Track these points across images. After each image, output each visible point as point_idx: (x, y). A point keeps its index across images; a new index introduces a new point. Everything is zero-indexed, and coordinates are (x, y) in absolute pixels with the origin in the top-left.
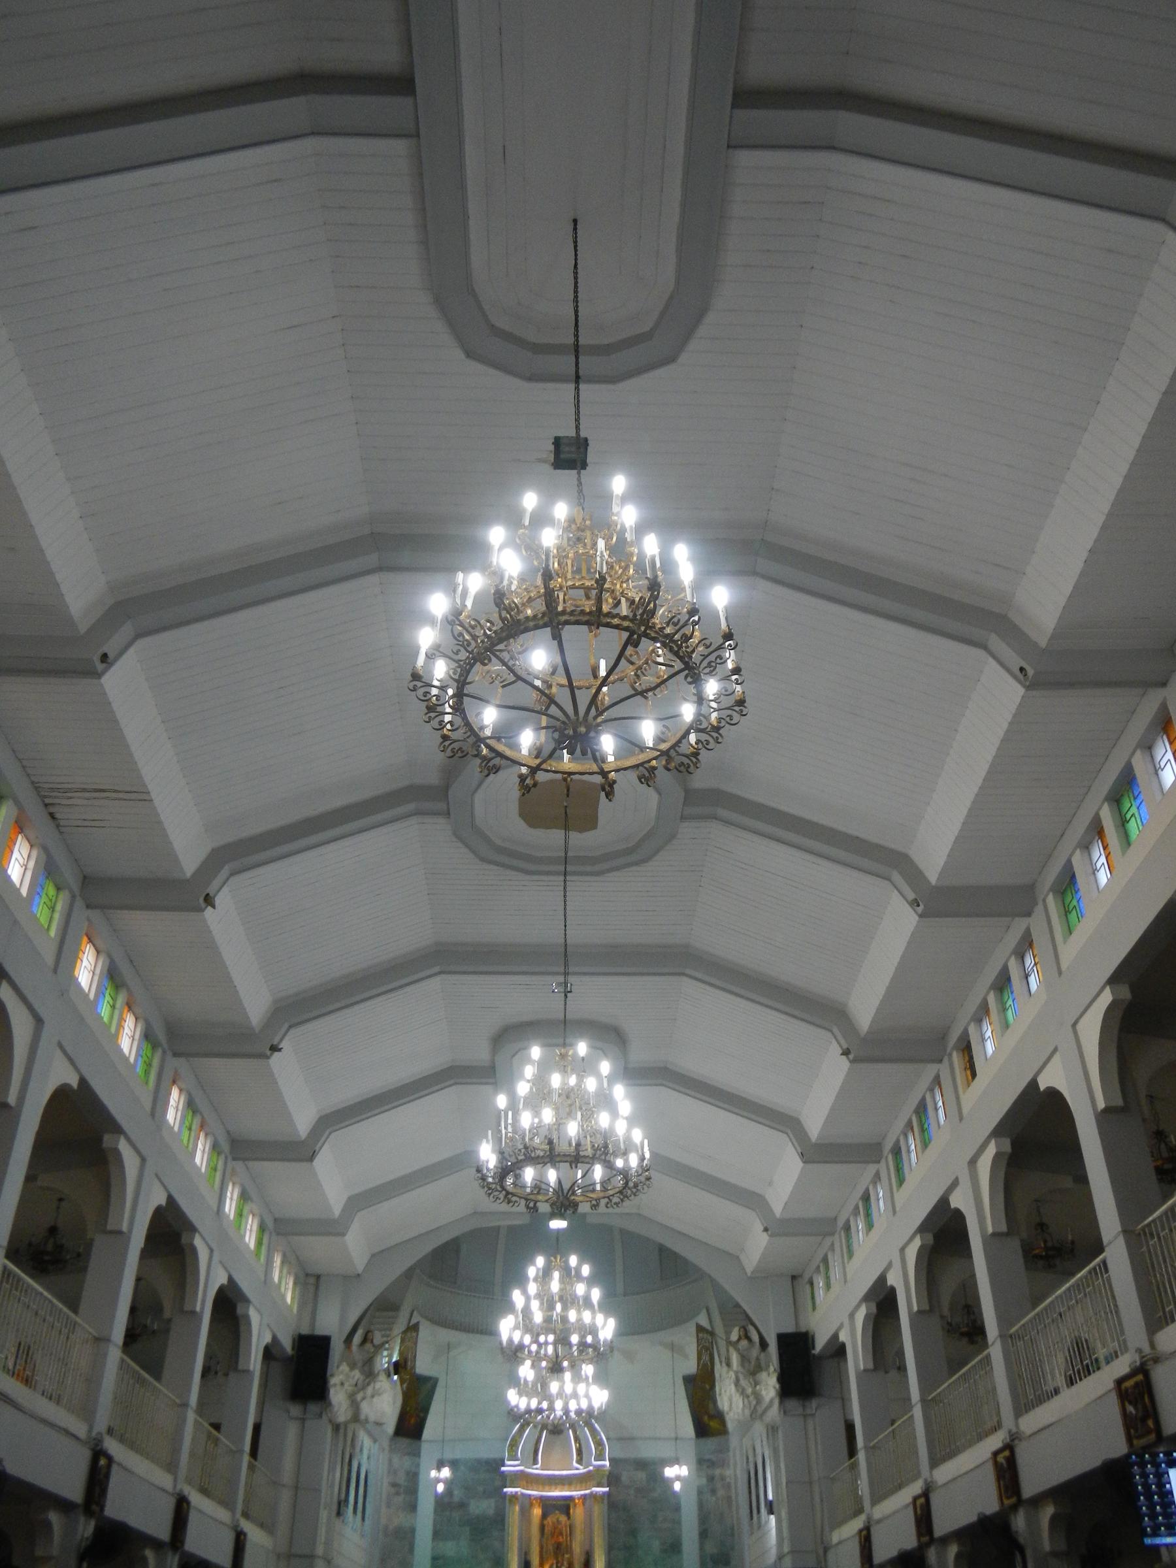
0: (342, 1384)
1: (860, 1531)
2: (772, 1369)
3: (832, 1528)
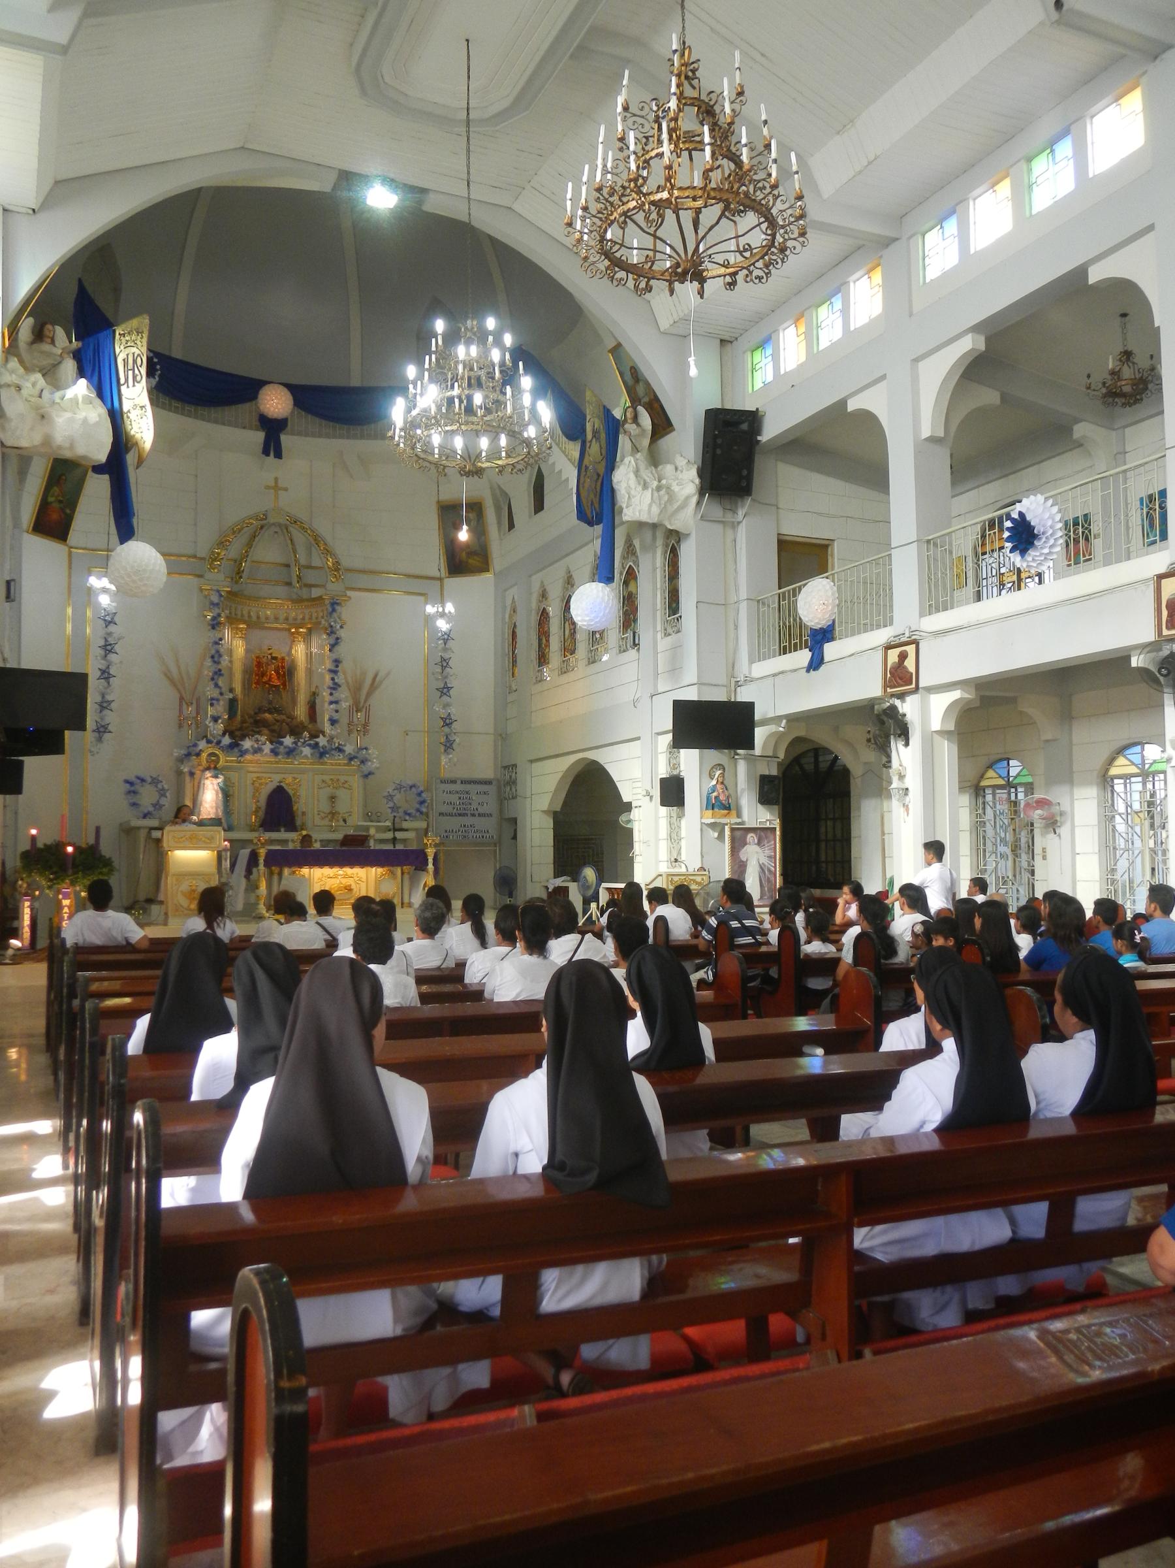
0: (19, 388)
1: (888, 647)
2: (681, 462)
3: (751, 662)
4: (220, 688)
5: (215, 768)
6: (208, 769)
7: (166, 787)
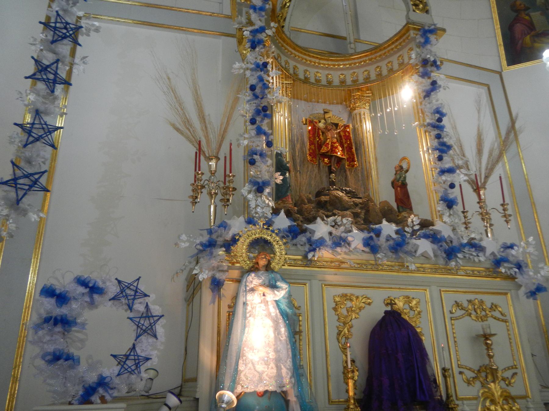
4: (265, 134)
5: (268, 268)
6: (254, 269)
7: (156, 310)
